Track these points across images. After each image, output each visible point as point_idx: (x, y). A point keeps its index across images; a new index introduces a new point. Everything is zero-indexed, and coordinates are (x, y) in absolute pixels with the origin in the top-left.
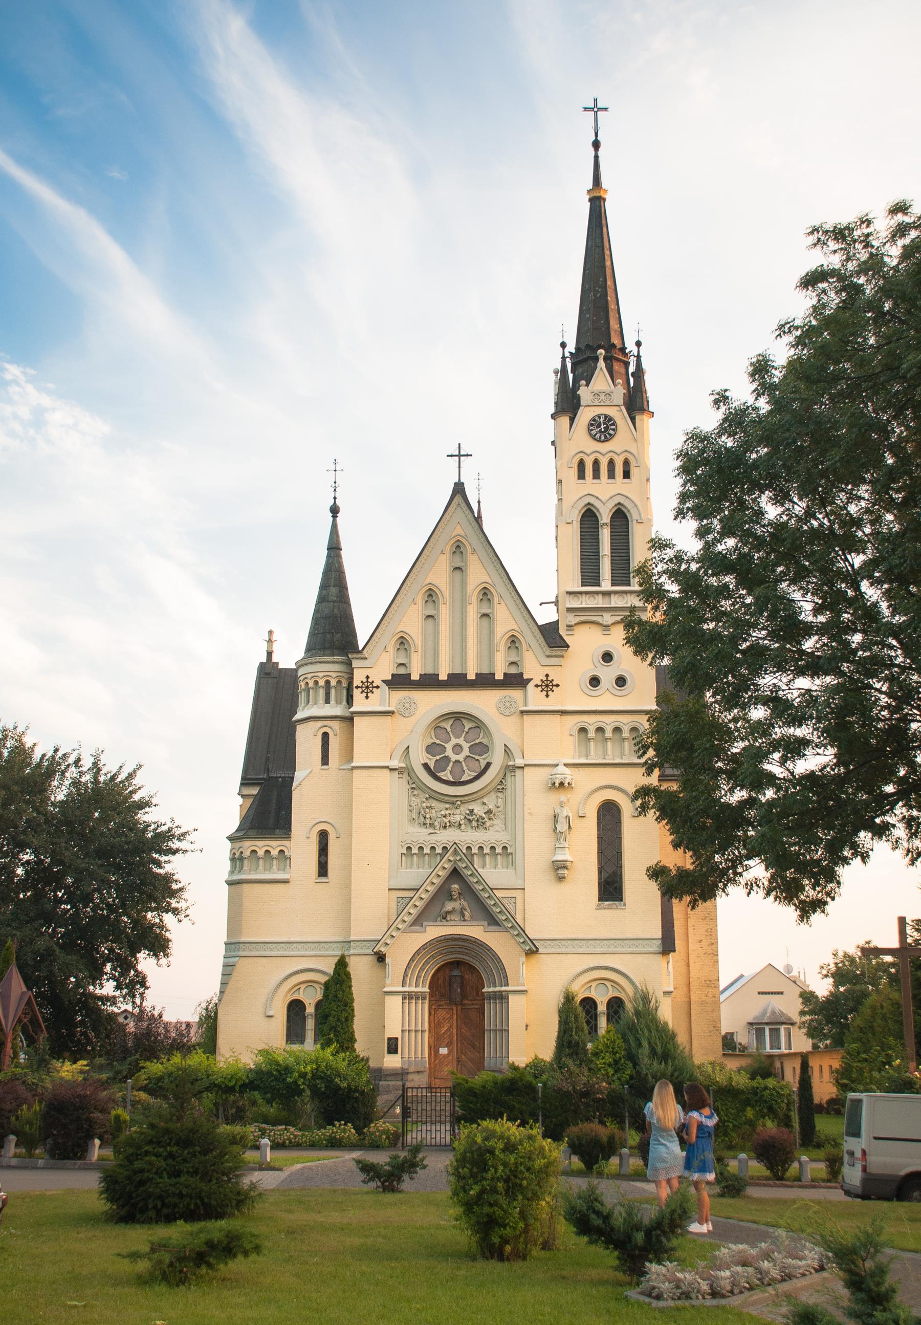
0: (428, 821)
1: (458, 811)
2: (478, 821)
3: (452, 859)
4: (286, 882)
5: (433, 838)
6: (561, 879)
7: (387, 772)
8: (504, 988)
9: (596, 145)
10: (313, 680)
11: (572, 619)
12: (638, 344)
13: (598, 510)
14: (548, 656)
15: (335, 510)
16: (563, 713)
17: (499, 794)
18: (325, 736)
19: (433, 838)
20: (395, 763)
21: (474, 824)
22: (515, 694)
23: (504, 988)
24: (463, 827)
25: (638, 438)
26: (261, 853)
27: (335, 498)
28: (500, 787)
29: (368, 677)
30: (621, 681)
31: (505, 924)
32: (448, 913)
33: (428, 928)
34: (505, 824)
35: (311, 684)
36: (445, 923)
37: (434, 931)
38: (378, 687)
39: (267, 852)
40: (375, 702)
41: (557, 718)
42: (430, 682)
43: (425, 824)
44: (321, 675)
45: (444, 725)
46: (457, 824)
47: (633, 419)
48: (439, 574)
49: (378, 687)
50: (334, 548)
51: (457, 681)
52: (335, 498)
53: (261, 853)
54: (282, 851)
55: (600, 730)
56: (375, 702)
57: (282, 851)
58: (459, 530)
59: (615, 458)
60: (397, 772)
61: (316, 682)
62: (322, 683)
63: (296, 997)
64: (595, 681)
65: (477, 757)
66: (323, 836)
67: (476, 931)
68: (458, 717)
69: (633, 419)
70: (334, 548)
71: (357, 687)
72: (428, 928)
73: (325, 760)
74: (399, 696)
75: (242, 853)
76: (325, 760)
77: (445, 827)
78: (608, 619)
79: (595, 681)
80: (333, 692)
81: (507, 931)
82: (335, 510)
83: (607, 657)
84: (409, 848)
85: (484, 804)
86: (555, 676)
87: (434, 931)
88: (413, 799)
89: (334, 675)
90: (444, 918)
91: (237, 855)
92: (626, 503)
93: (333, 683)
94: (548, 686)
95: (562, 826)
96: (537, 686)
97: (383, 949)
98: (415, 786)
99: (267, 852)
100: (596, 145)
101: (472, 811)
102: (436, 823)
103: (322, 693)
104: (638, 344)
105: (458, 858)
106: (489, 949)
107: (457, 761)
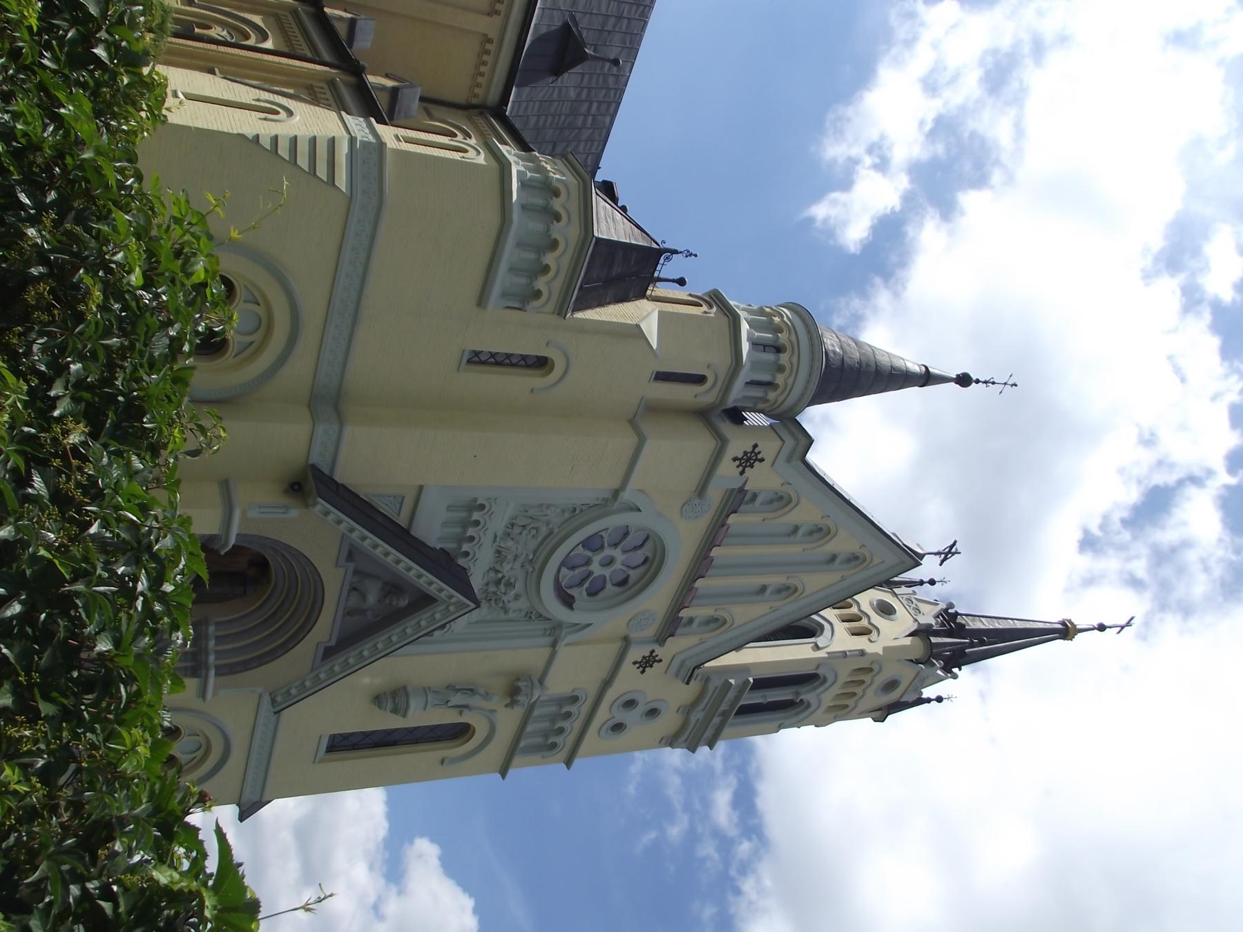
0: (517, 530)
1: (517, 565)
2: (495, 593)
3: (453, 600)
4: (481, 301)
5: (487, 540)
6: (378, 700)
7: (615, 483)
8: (212, 672)
9: (1102, 628)
10: (787, 365)
11: (716, 683)
12: (939, 699)
13: (815, 689)
14: (683, 662)
15: (964, 380)
16: (607, 684)
17: (523, 613)
18: (700, 379)
19: (487, 540)
20: (626, 496)
21: (492, 588)
22: (651, 631)
23: (212, 672)
24: (492, 574)
25: (861, 715)
26: (549, 259)
27: (977, 381)
28: (532, 615)
29: (762, 460)
30: (618, 727)
31: (327, 667)
32: (364, 597)
33: (341, 571)
34: (477, 622)
35: (784, 358)
36: (346, 588)
37: (333, 579)
38: (742, 473)
39: (546, 269)
40: (727, 468)
41: (603, 674)
42: (715, 534)
43: (513, 525)
44: (790, 381)
45: (649, 545)
46: (498, 568)
47: (880, 709)
48: (843, 543)
49: (742, 473)
50: (927, 378)
51: (701, 564)
52: (977, 381)
53: (549, 259)
54: (537, 294)
55: (568, 715)
56: (727, 468)
57: (537, 294)
58: (876, 561)
59: (856, 698)
60: (608, 495)
61: (781, 369)
62: (780, 379)
63: (240, 292)
64: (630, 704)
65: (587, 585)
66: (541, 363)
67: (323, 630)
68: (653, 565)
69: (880, 709)
70: (927, 378)
71: (755, 446)
72: (341, 571)
73: (663, 377)
74: (715, 494)
75: (557, 217)
76: (663, 377)
77: (499, 552)
78: (698, 715)
79: (630, 704)
80: (757, 392)
81: (313, 670)
82: (964, 380)
83: (653, 713)
84: (482, 507)
85: (517, 597)
86: (654, 671)
87: (333, 579)
88: (558, 510)
89: (780, 400)
90: (355, 589)
91: (557, 204)
92: (806, 713)
93: (772, 395)
94: (647, 663)
95: (457, 699)
96: (653, 651)
97: (318, 507)
98: (577, 514)
99: (546, 269)
100: (1102, 628)
101: (510, 585)
102: (510, 543)
103: (765, 377)
104: (939, 699)
105: (452, 608)
106: (286, 647)
107: (588, 562)
